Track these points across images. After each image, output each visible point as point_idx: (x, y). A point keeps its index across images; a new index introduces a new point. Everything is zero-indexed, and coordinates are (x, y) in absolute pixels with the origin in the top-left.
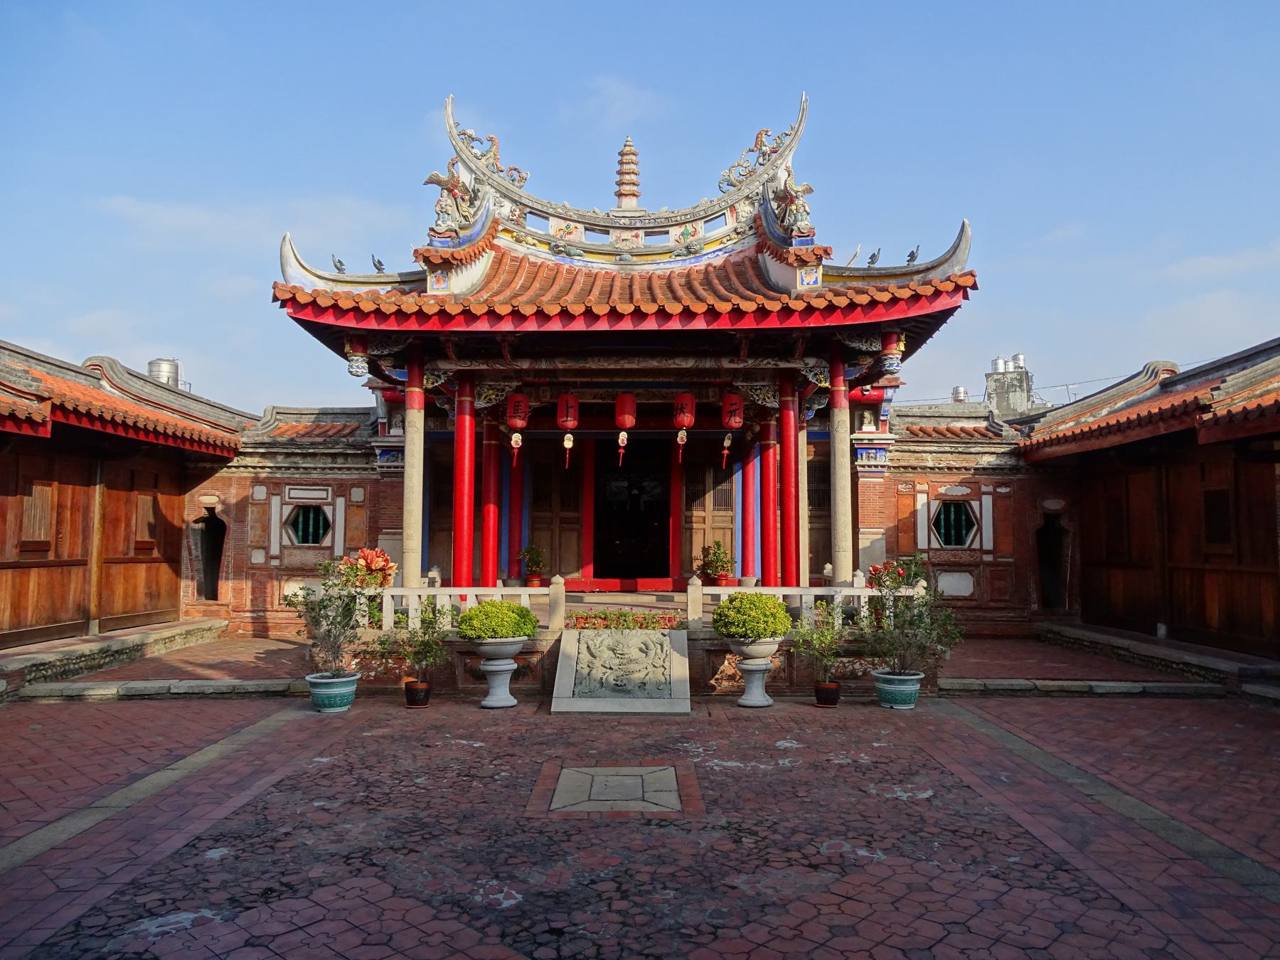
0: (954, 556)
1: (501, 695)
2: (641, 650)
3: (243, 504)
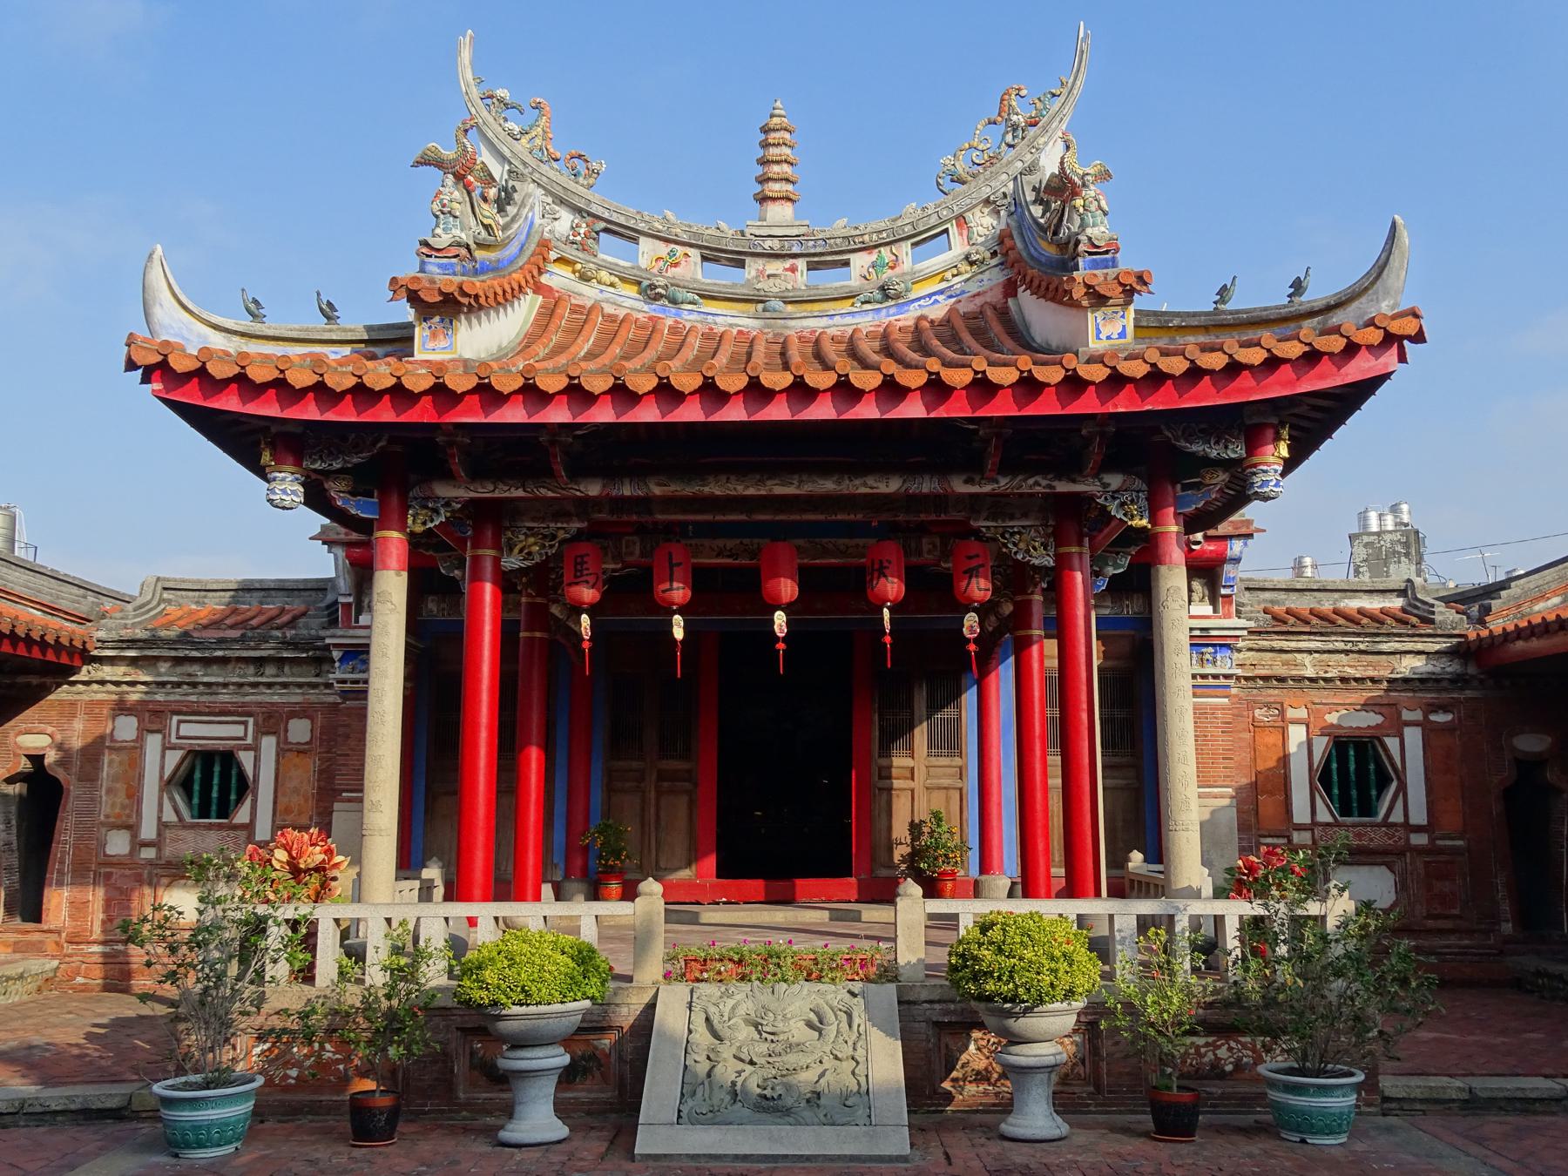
0: (1359, 836)
1: (538, 1120)
2: (810, 1025)
3: (94, 751)
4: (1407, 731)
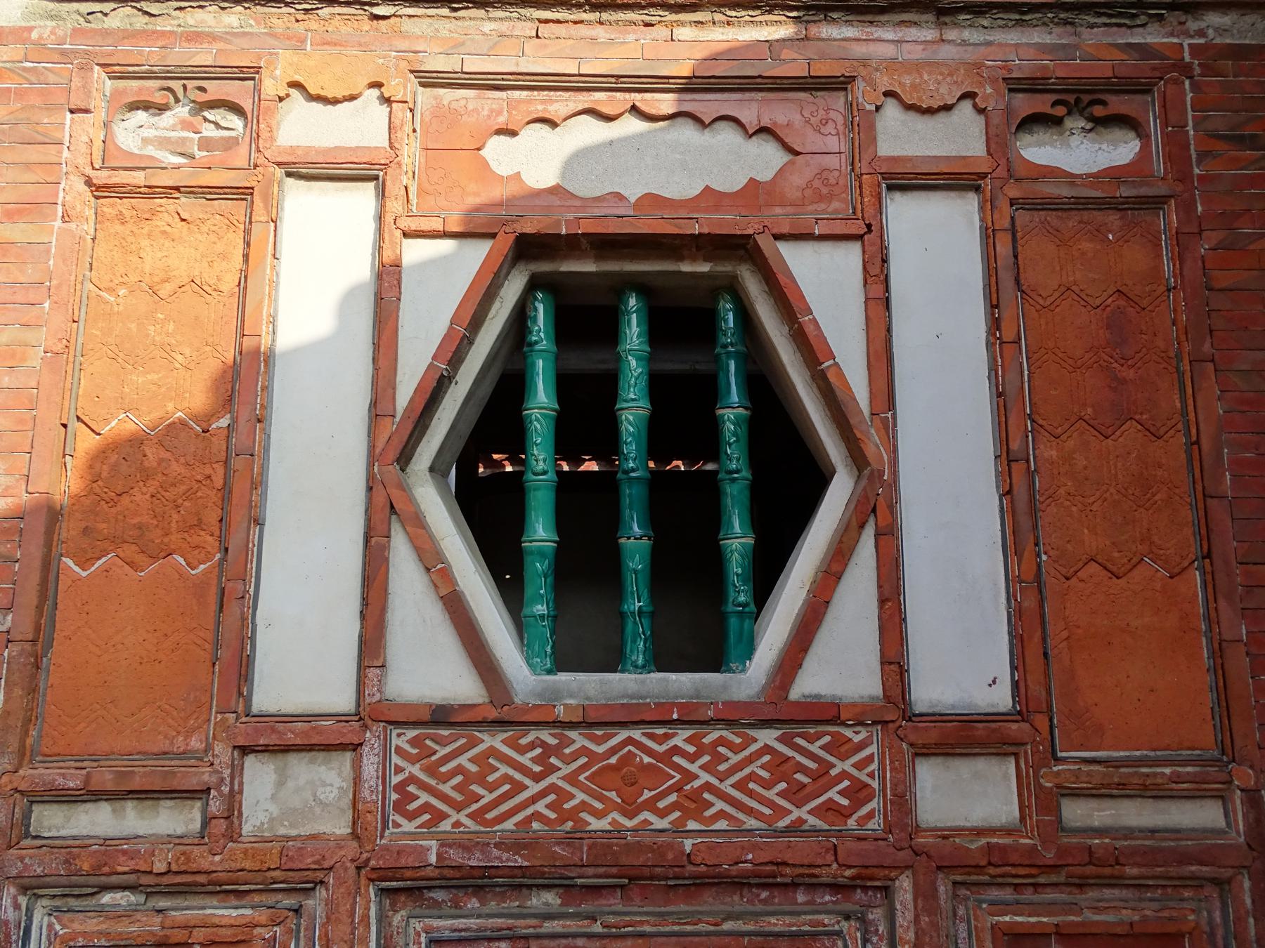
0: (625, 780)
4: (906, 217)
